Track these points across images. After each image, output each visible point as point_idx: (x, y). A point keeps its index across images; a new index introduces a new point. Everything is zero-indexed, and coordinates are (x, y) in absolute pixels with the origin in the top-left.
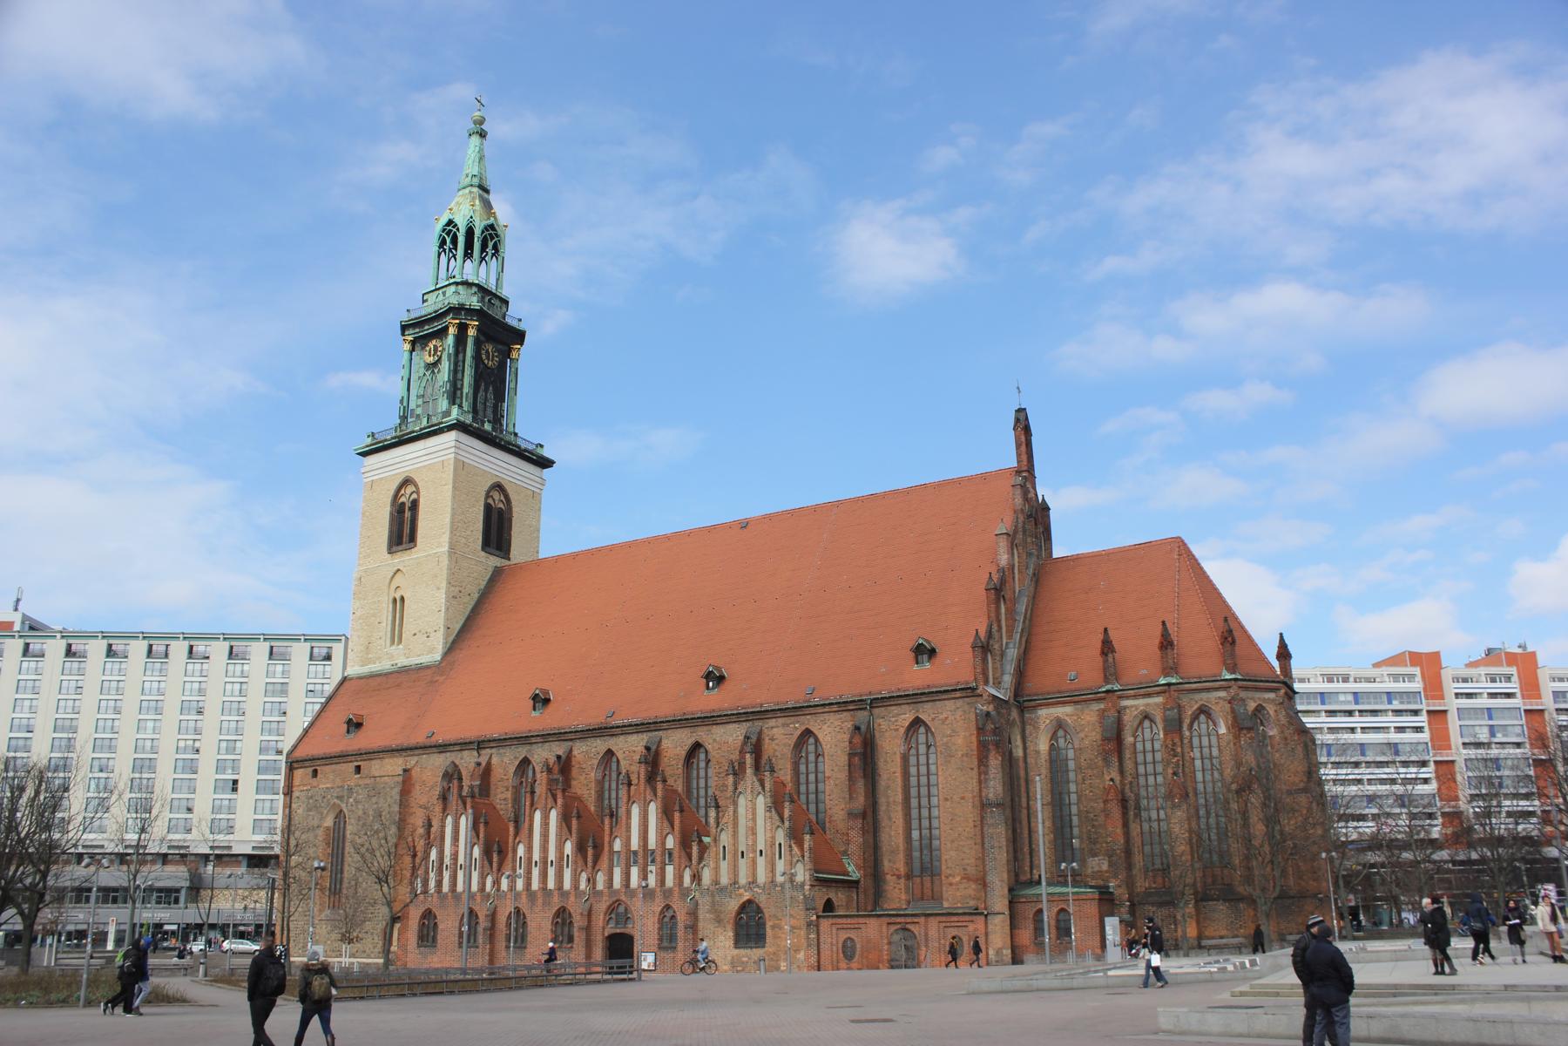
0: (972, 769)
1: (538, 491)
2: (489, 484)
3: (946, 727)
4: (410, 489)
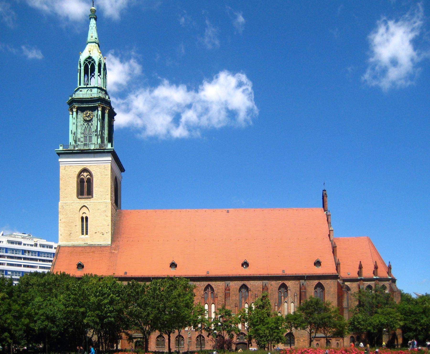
0: (335, 298)
3: (328, 285)
4: (85, 174)
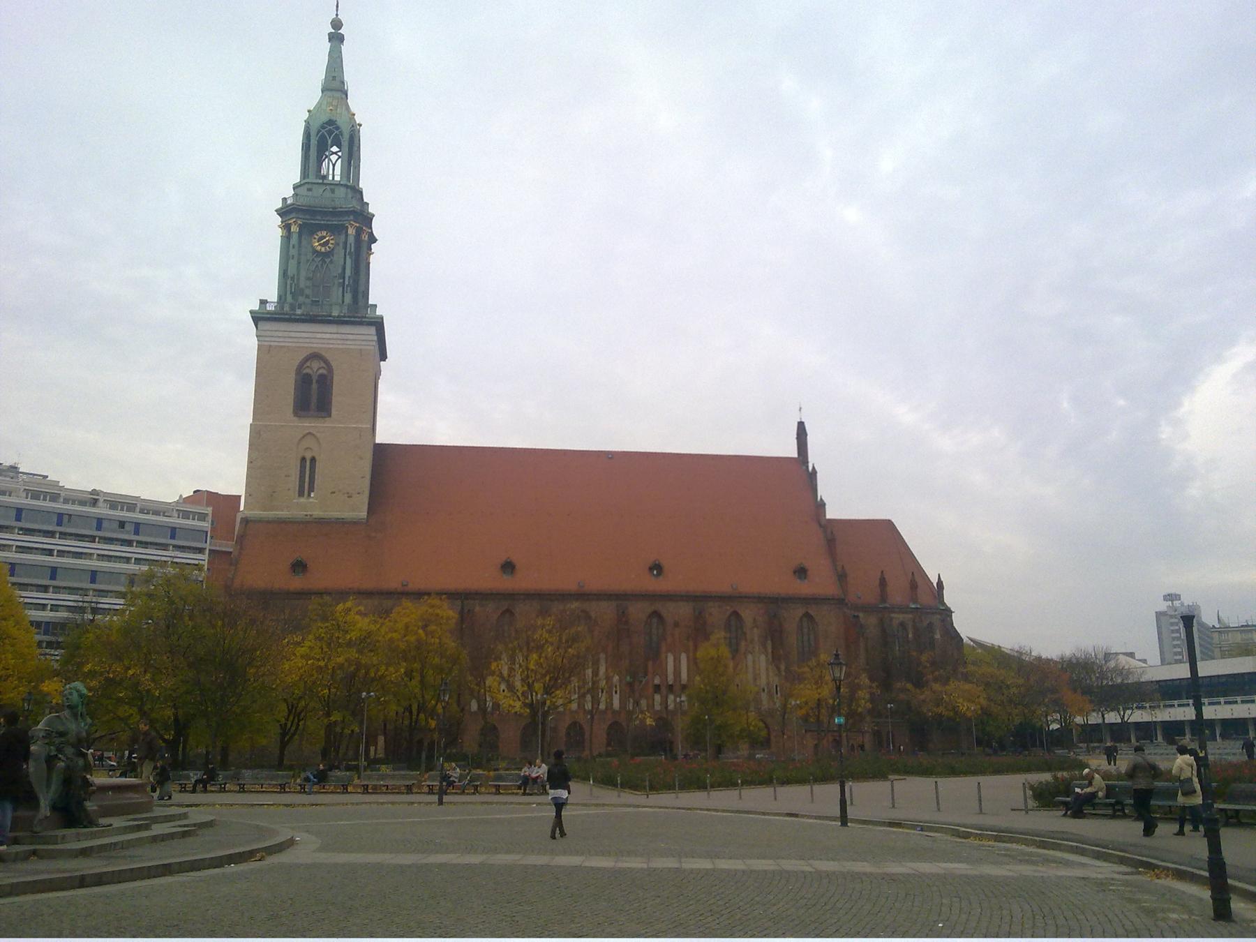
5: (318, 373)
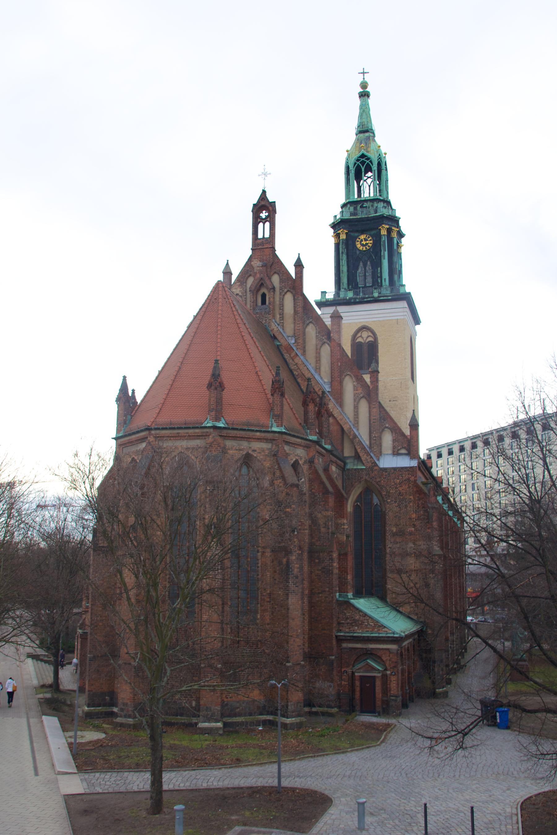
1: (402, 317)
2: (354, 330)
5: (367, 341)
